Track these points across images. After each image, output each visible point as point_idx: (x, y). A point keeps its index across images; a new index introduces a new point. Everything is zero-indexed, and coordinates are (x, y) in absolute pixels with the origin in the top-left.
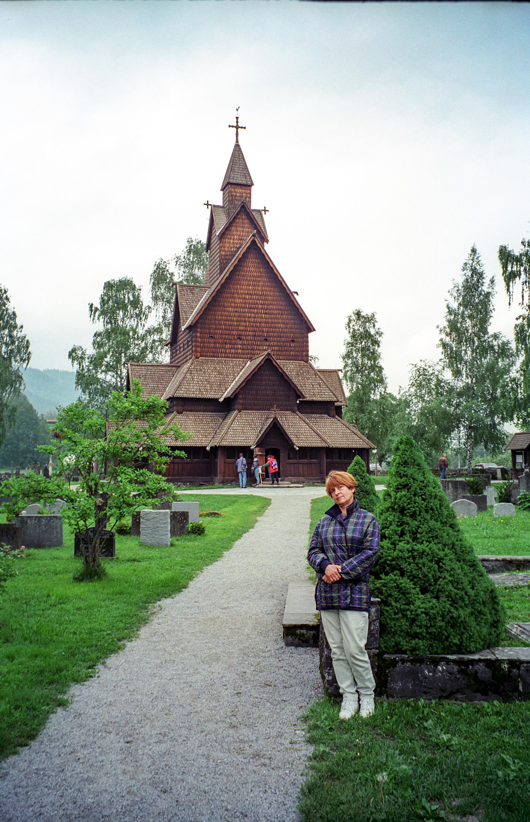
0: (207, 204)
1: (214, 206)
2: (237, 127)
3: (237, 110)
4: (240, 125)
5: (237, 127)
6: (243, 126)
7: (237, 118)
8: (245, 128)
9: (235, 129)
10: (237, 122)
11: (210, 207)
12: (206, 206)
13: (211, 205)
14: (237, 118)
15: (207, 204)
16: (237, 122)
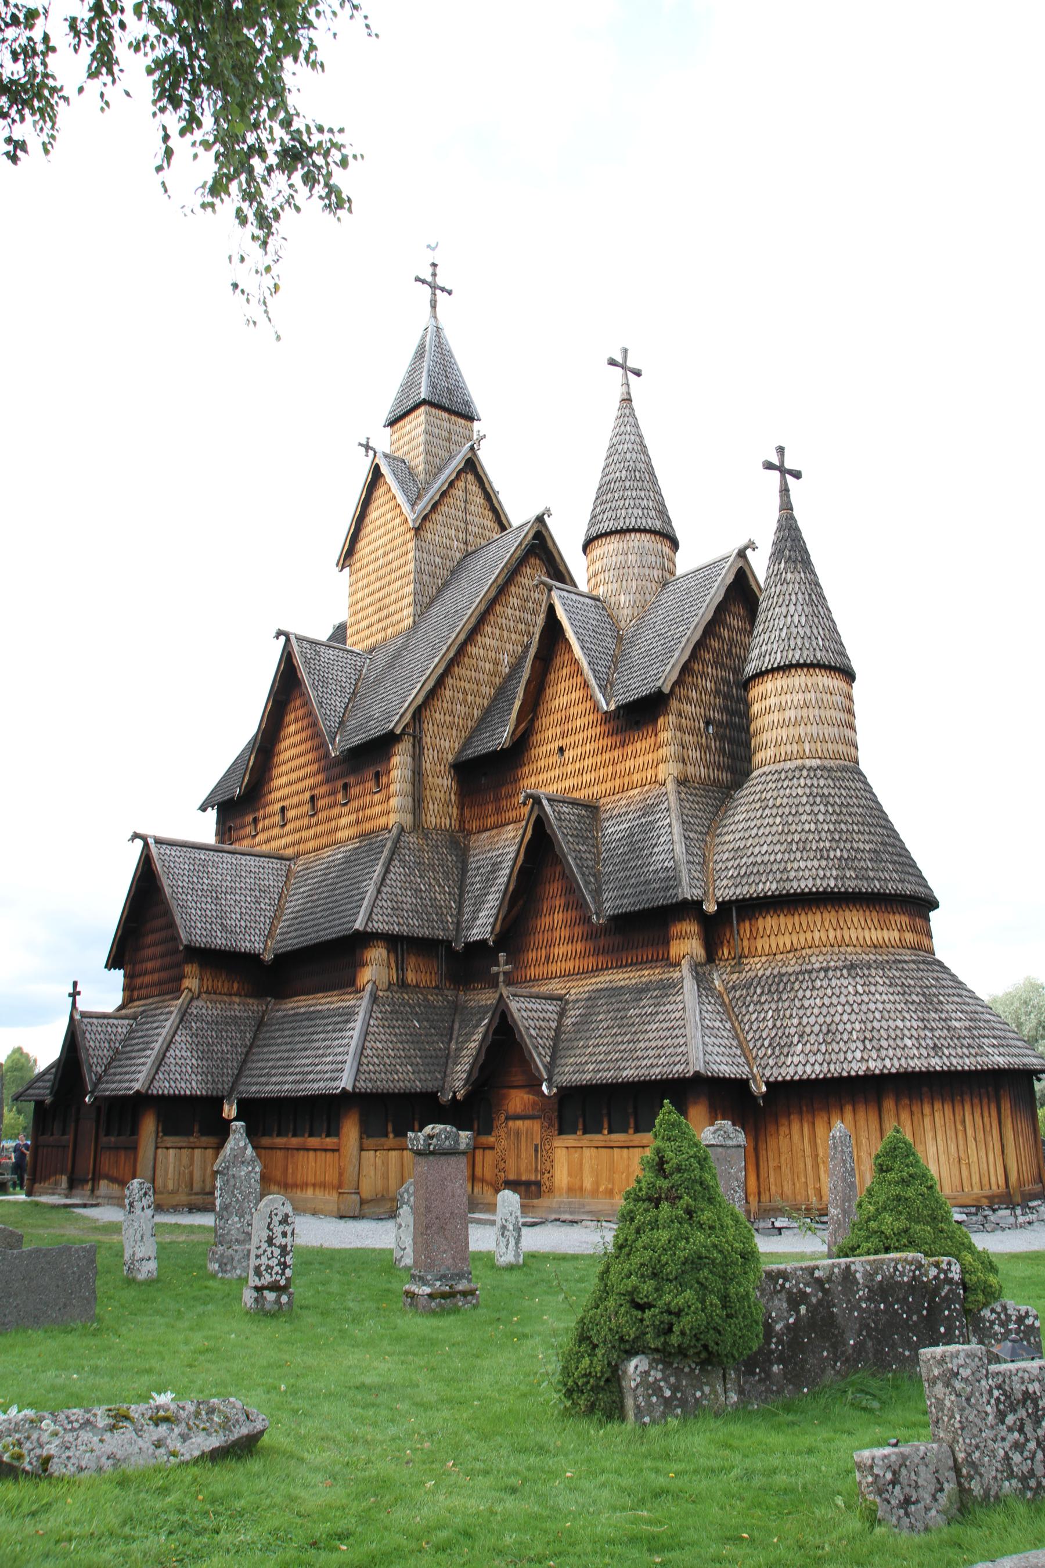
0: (367, 447)
1: (386, 456)
2: (434, 287)
3: (433, 249)
4: (440, 281)
5: (434, 287)
6: (448, 288)
7: (434, 265)
8: (450, 293)
9: (427, 290)
10: (434, 275)
11: (371, 453)
12: (363, 449)
13: (372, 449)
14: (434, 265)
15: (367, 447)
16: (434, 275)
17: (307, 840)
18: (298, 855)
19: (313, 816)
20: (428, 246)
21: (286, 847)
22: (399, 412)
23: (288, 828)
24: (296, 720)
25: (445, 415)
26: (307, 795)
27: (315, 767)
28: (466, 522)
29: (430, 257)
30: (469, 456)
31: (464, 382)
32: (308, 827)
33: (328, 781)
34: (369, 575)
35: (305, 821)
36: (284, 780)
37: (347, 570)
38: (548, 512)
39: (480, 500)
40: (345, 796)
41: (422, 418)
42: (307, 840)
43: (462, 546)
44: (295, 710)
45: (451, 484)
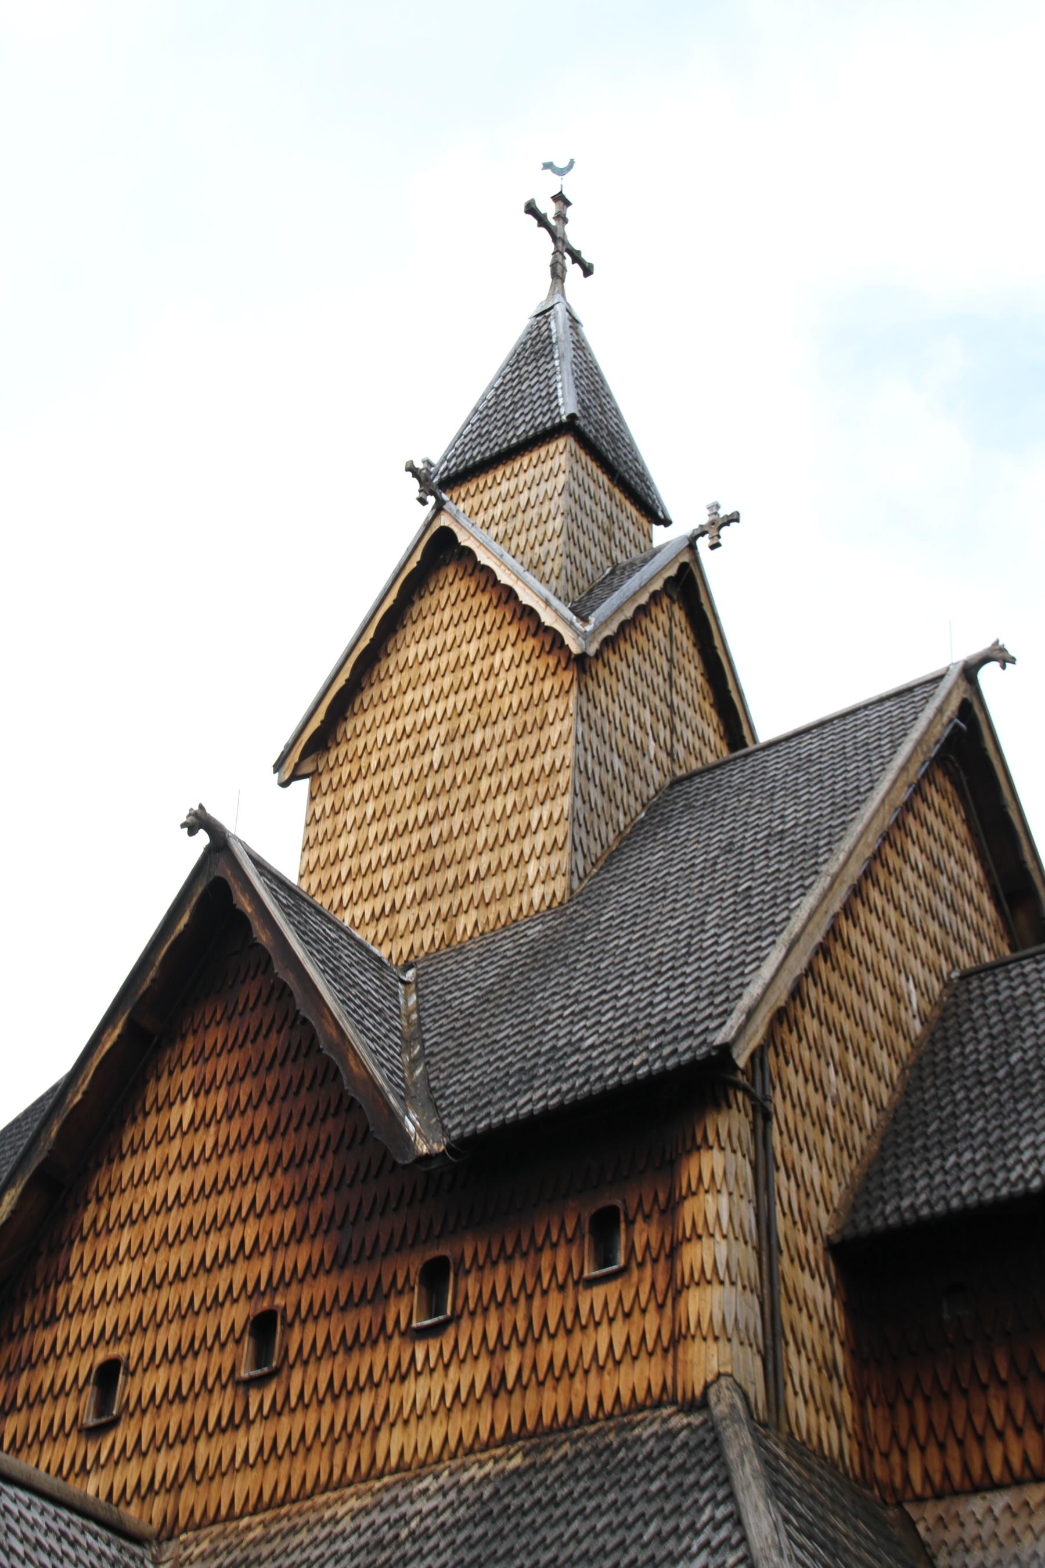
11: (431, 500)
12: (415, 484)
17: (220, 1471)
18: (169, 1530)
19: (259, 1382)
20: (548, 166)
21: (146, 1492)
22: (476, 455)
23: (125, 1434)
24: (202, 1088)
25: (603, 479)
26: (237, 1314)
27: (286, 1220)
28: (671, 706)
29: (553, 184)
30: (686, 558)
31: (630, 439)
32: (231, 1425)
33: (341, 1262)
34: (386, 789)
35: (221, 1404)
36: (124, 1273)
37: (302, 786)
38: (999, 655)
39: (693, 669)
40: (434, 1306)
41: (562, 460)
42: (220, 1471)
43: (663, 756)
44: (200, 1057)
45: (642, 610)
